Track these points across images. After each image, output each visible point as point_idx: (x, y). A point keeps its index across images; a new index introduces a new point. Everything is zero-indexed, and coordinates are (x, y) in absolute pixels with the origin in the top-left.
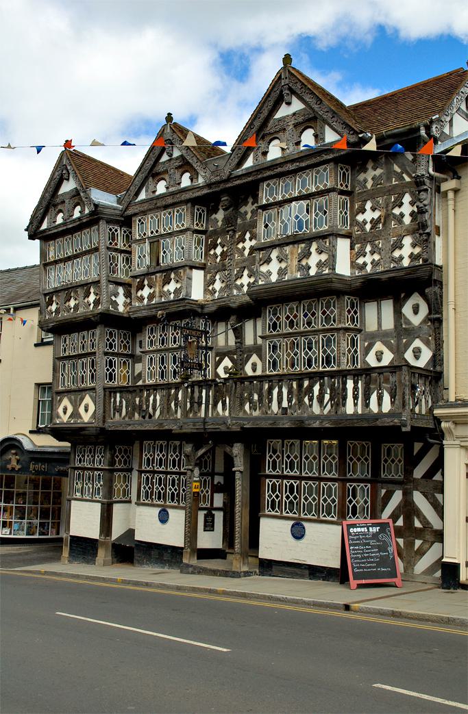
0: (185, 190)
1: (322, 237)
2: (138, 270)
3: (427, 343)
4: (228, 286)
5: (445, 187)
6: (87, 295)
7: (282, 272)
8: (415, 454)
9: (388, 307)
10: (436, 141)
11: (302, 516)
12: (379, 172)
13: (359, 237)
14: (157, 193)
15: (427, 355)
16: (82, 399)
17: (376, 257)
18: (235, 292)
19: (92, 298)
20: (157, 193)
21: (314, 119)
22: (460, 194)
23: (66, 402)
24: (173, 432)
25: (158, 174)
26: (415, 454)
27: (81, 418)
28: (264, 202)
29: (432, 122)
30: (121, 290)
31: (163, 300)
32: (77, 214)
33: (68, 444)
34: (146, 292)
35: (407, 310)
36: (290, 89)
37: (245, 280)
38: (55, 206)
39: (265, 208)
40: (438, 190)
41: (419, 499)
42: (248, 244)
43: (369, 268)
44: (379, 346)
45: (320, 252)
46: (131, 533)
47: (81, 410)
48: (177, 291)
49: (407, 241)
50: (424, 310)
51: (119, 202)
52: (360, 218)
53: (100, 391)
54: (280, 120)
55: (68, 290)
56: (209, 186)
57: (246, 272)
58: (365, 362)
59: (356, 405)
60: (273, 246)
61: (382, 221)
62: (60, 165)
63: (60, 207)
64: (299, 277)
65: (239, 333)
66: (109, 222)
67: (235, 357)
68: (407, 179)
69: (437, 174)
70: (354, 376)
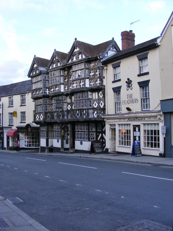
0: (58, 67)
1: (83, 79)
2: (51, 85)
3: (103, 102)
4: (68, 89)
5: (105, 68)
6: (40, 91)
7: (76, 86)
9: (97, 93)
10: (102, 59)
11: (82, 140)
12: (94, 64)
13: (90, 78)
14: (54, 67)
15: (103, 104)
17: (93, 83)
18: (69, 90)
19: (41, 92)
20: (54, 67)
22: (107, 70)
23: (38, 116)
25: (54, 63)
28: (73, 70)
29: (100, 55)
30: (47, 89)
32: (37, 72)
33: (38, 126)
34: (52, 90)
35: (100, 94)
36: (76, 46)
37: (71, 87)
38: (33, 70)
39: (73, 72)
40: (103, 69)
41: (104, 134)
42: (71, 79)
43: (92, 85)
44: (95, 102)
46: (52, 145)
47: (40, 117)
48: (58, 90)
49: (98, 80)
51: (46, 69)
52: (90, 74)
53: (44, 113)
54: (75, 52)
55: (36, 90)
56: (63, 66)
57: (71, 85)
58: (93, 106)
59: (91, 116)
60: (75, 81)
62: (34, 61)
65: (71, 98)
66: (44, 74)
69: (103, 66)
70: (91, 110)
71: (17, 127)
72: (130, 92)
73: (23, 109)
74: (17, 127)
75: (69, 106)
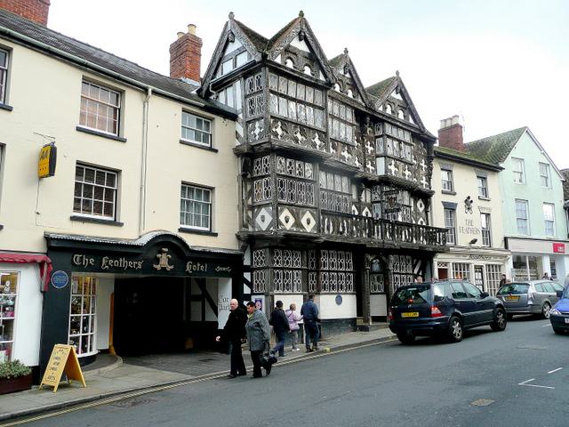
16: (304, 214)
23: (286, 213)
27: (302, 227)
47: (304, 222)
50: (423, 206)
71: (48, 239)
72: (468, 216)
73: (102, 153)
74: (48, 239)
75: (354, 208)
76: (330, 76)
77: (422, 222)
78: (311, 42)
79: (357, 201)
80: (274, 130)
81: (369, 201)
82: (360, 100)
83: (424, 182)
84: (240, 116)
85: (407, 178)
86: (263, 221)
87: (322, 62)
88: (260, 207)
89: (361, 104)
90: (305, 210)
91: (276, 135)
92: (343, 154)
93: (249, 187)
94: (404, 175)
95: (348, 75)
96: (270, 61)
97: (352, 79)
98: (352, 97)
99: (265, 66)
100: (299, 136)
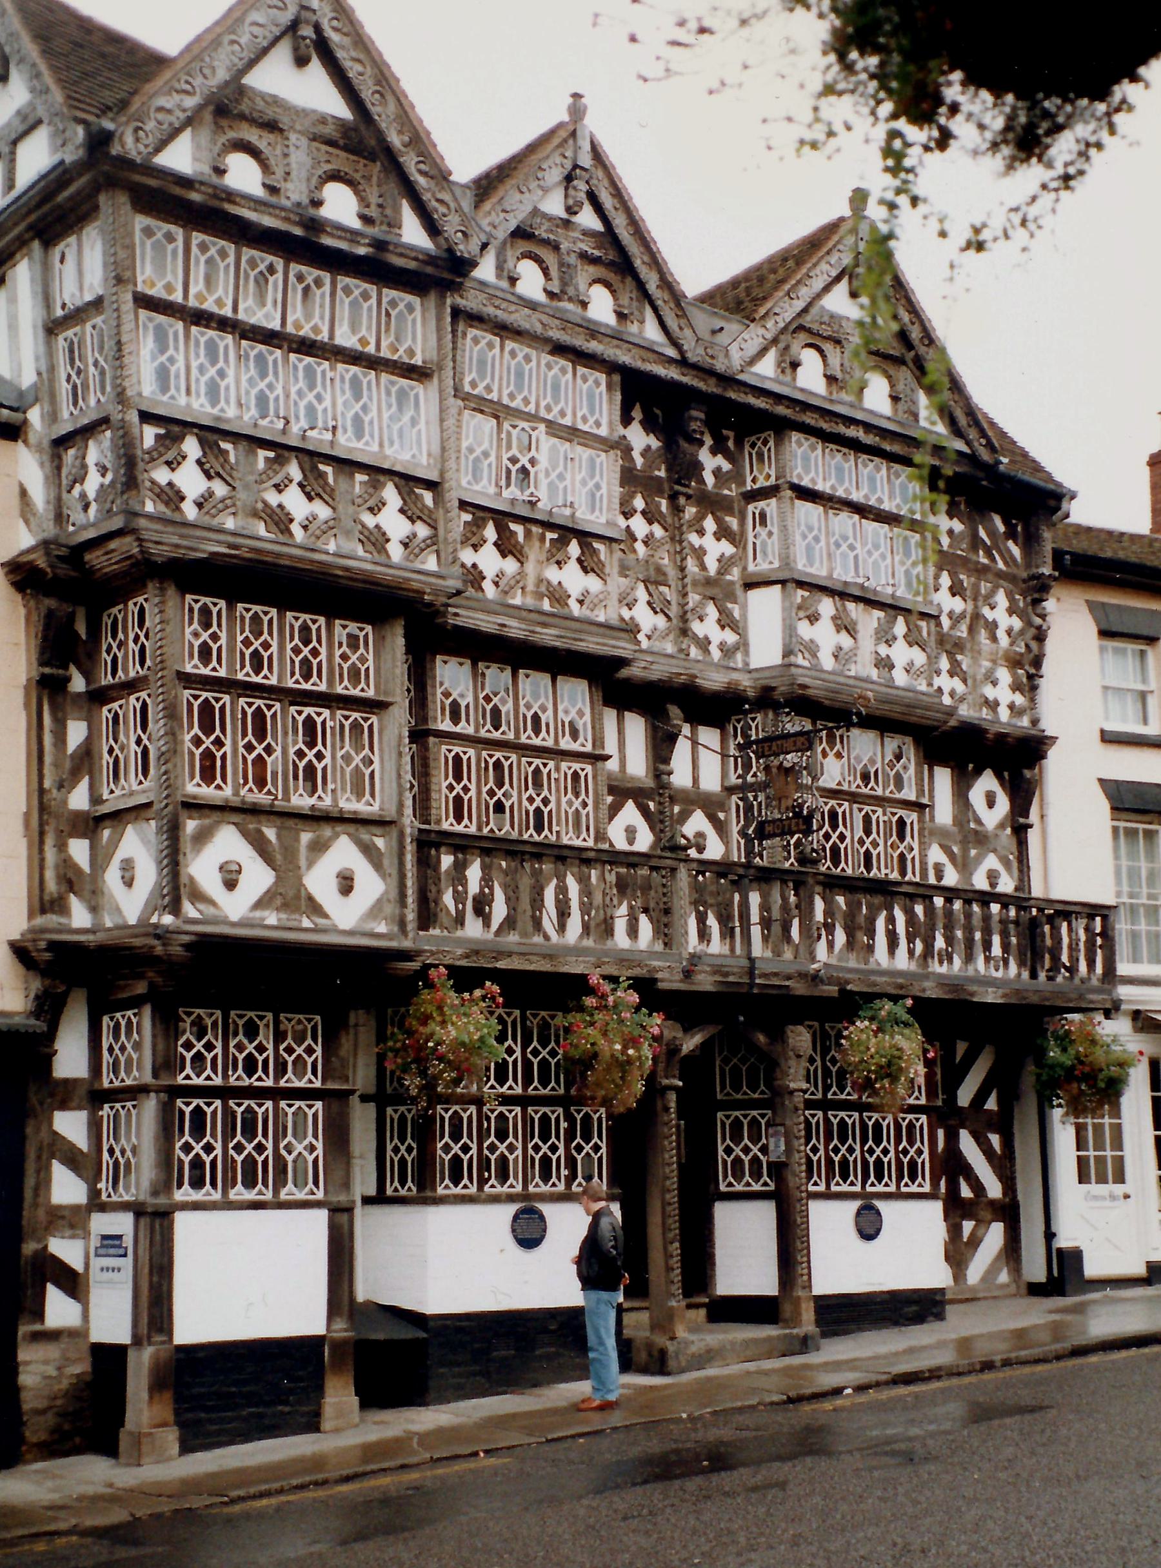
3: (1006, 863)
8: (958, 1059)
21: (899, 361)
24: (661, 985)
26: (958, 1059)
27: (315, 908)
31: (546, 605)
41: (967, 1145)
45: (912, 640)
50: (1003, 804)
61: (968, 620)
63: (252, 135)
64: (875, 677)
67: (651, 805)
68: (1001, 565)
75: (630, 814)
76: (451, 226)
77: (992, 876)
78: (353, 70)
79: (650, 783)
80: (162, 476)
81: (711, 782)
82: (651, 332)
83: (1003, 692)
84: (34, 416)
85: (900, 678)
86: (129, 883)
87: (410, 162)
88: (118, 817)
89: (649, 349)
90: (327, 831)
91: (172, 496)
92: (553, 574)
93: (76, 732)
94: (885, 664)
95: (587, 219)
96: (125, 163)
97: (610, 235)
98: (610, 319)
99: (111, 183)
100: (295, 502)
